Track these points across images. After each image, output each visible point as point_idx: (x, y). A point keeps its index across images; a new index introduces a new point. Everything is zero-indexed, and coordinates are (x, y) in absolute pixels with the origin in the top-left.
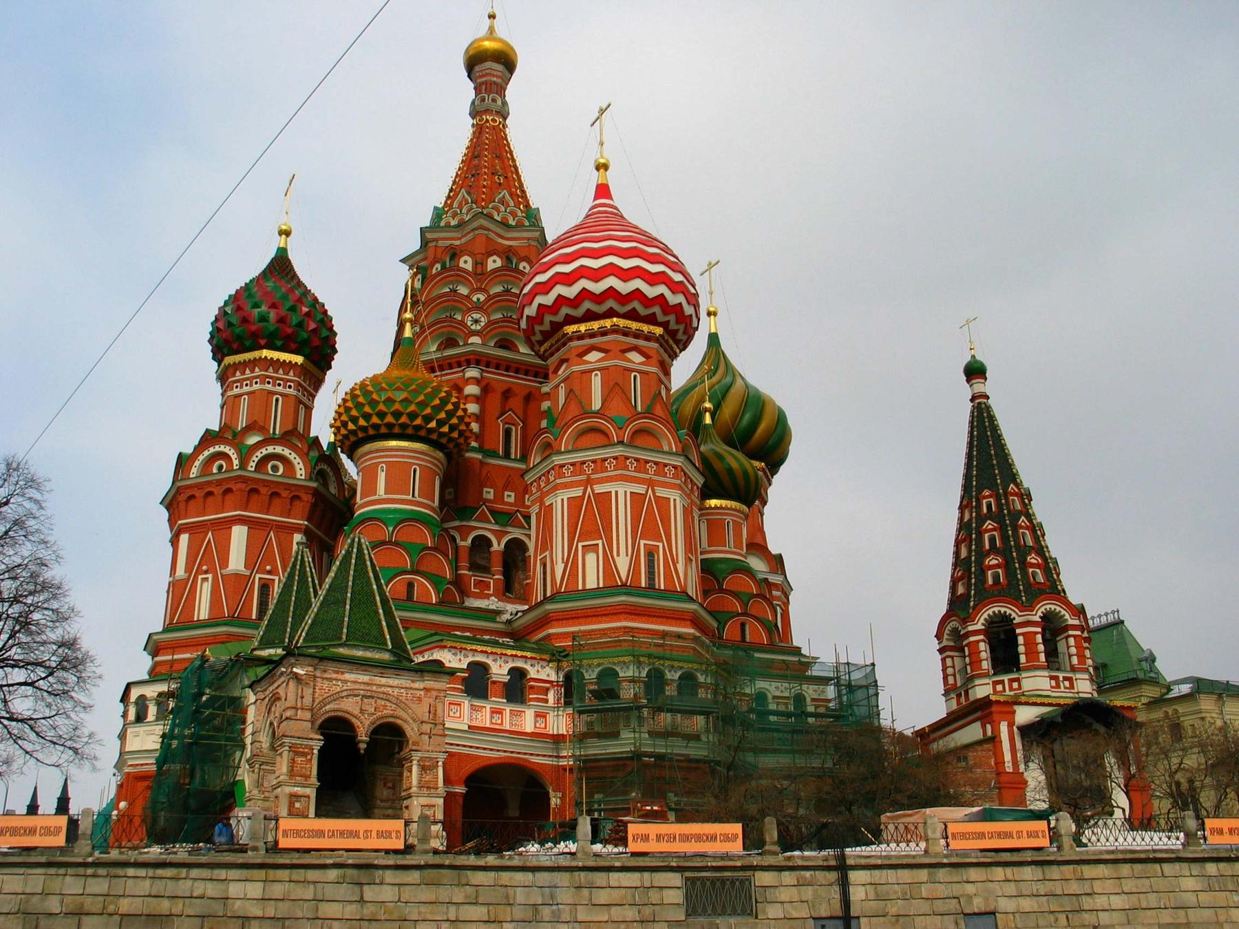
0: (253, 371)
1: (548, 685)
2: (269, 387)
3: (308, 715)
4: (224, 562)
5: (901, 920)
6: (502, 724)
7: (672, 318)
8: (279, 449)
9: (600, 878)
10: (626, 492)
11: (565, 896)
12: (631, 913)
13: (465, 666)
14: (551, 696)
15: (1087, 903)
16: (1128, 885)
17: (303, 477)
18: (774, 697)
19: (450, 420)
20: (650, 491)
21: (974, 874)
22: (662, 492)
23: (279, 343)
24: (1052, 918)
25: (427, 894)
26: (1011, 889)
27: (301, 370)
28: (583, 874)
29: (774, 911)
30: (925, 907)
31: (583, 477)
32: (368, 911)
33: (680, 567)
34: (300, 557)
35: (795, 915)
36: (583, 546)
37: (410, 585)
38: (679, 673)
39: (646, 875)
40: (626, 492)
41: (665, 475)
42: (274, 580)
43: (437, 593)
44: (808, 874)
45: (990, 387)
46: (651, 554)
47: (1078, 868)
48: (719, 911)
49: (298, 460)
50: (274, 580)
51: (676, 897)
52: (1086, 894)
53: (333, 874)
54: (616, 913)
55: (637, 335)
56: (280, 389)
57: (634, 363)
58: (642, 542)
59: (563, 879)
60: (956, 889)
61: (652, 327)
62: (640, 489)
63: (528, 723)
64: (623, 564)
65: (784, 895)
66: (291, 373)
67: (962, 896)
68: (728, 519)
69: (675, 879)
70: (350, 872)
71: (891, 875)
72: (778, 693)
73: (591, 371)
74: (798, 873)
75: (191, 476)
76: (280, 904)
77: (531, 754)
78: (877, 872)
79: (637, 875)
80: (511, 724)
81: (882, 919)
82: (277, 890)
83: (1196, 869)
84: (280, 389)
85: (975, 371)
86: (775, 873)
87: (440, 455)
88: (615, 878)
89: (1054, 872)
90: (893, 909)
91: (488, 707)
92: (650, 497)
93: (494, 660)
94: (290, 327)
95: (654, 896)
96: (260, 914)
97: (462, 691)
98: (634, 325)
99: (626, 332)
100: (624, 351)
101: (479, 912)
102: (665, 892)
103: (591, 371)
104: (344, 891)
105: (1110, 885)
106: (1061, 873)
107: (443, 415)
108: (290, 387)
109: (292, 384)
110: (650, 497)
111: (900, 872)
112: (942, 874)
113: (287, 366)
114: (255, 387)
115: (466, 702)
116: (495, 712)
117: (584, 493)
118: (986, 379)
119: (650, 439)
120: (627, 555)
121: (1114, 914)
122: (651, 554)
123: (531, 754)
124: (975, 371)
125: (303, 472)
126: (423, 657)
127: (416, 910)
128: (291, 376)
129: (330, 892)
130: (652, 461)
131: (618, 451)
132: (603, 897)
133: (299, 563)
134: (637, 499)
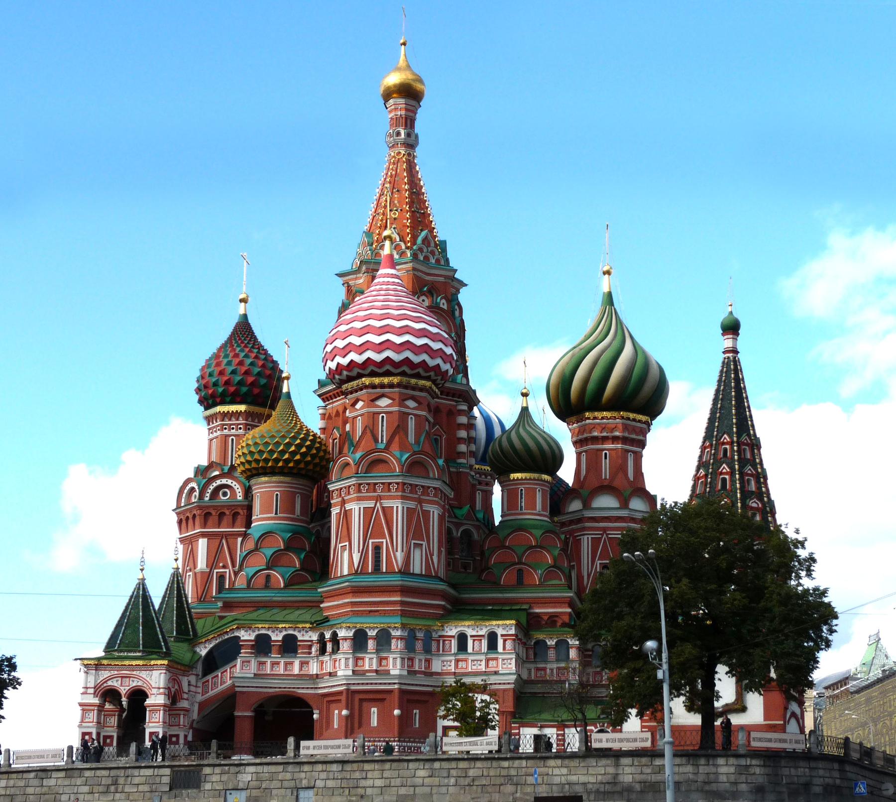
0: (216, 422)
1: (310, 643)
2: (226, 432)
3: (92, 691)
4: (195, 567)
5: (266, 790)
6: (279, 671)
7: (405, 368)
8: (224, 481)
9: (136, 772)
10: (360, 508)
11: (121, 781)
12: (146, 788)
13: (253, 638)
14: (313, 649)
15: (363, 783)
16: (387, 774)
17: (241, 498)
18: (471, 636)
19: (310, 452)
20: (378, 504)
21: (306, 768)
22: (387, 503)
23: (228, 399)
24: (342, 790)
25: (67, 782)
26: (323, 775)
27: (247, 415)
28: (130, 770)
29: (208, 786)
30: (279, 785)
31: (340, 499)
32: (45, 790)
33: (400, 555)
34: (176, 579)
35: (217, 788)
36: (341, 546)
37: (268, 577)
38: (376, 631)
39: (156, 770)
40: (360, 508)
41: (389, 490)
42: (226, 572)
43: (284, 580)
44: (227, 768)
45: (743, 342)
46: (377, 549)
47: (362, 764)
48: (195, 786)
49: (238, 486)
50: (226, 572)
51: (166, 780)
52: (362, 778)
53: (32, 775)
54: (141, 788)
55: (382, 386)
56: (233, 432)
57: (381, 407)
58: (371, 541)
59: (121, 773)
60: (296, 776)
61: (391, 378)
62: (371, 504)
63: (296, 670)
64: (356, 557)
65: (215, 778)
66: (241, 419)
67: (298, 779)
68: (522, 487)
69: (167, 771)
70: (40, 773)
71: (266, 769)
72: (474, 633)
73: (357, 417)
74: (222, 767)
75: (182, 505)
76: (12, 789)
77: (298, 688)
78: (259, 767)
79: (152, 770)
80: (286, 669)
81: (258, 790)
82: (11, 783)
83: (427, 765)
84: (233, 432)
85: (732, 328)
86: (212, 768)
87: (302, 481)
88: (145, 772)
89: (348, 767)
90: (264, 786)
91: (269, 661)
92: (378, 508)
93: (272, 632)
94: (233, 386)
95: (158, 780)
96: (4, 793)
97: (251, 653)
98: (377, 380)
99: (373, 386)
100: (373, 400)
101: (86, 789)
102: (163, 778)
103: (357, 417)
104: (36, 782)
105: (377, 774)
106: (352, 767)
107: (304, 450)
108: (240, 428)
109: (241, 426)
110: (378, 508)
111: (270, 767)
112: (290, 768)
113: (237, 415)
114: (219, 433)
115: (253, 660)
116: (273, 664)
117: (341, 510)
118: (738, 334)
119: (381, 466)
120: (359, 552)
121: (375, 789)
122: (377, 549)
123: (298, 688)
124: (732, 328)
125: (241, 494)
126: (228, 635)
127: (62, 789)
128: (241, 421)
129: (32, 782)
130: (380, 483)
131: (352, 481)
132: (136, 780)
133: (175, 582)
134: (368, 512)
